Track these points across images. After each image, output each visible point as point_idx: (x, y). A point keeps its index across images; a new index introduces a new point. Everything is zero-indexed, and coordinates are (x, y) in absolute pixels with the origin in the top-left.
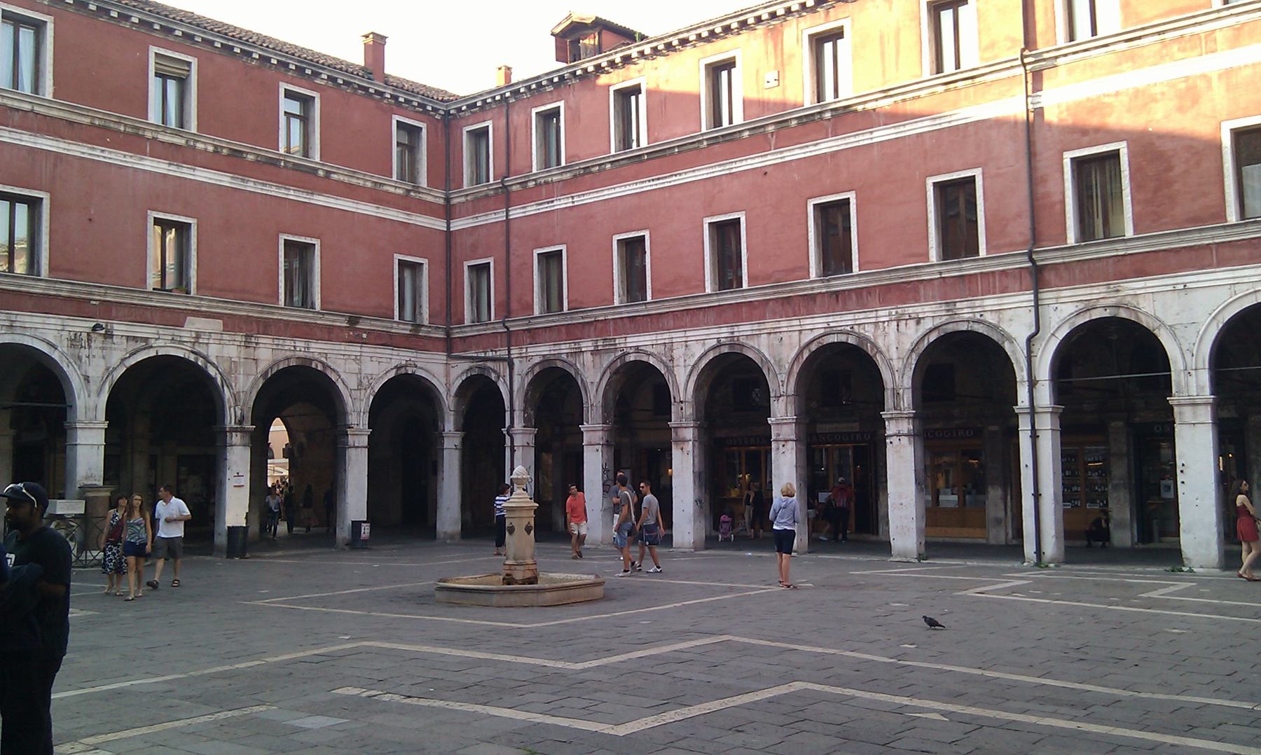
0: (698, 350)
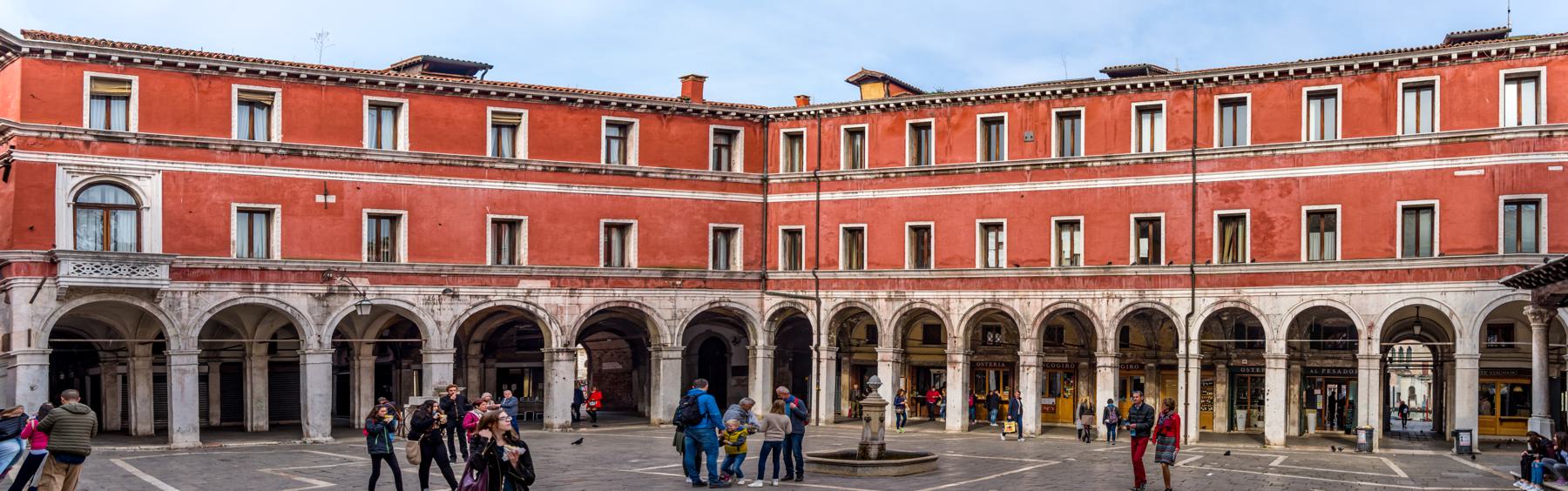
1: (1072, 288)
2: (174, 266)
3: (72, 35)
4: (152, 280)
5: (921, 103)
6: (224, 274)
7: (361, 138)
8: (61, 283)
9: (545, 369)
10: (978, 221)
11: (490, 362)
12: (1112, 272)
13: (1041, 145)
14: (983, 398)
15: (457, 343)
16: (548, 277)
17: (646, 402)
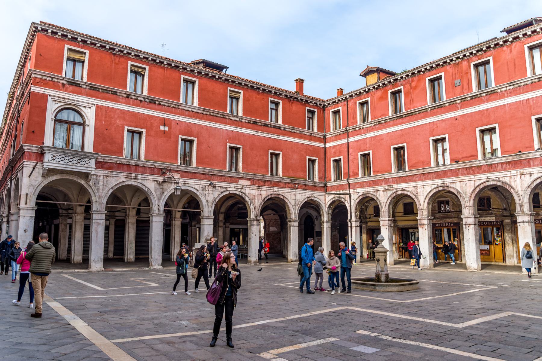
0: (428, 189)
1: (494, 171)
2: (97, 160)
3: (62, 27)
4: (87, 167)
5: (396, 80)
6: (120, 166)
7: (180, 97)
8: (45, 166)
9: (249, 230)
10: (431, 139)
11: (227, 224)
12: (522, 157)
13: (466, 86)
14: (441, 246)
15: (215, 214)
16: (250, 179)
17: (286, 249)
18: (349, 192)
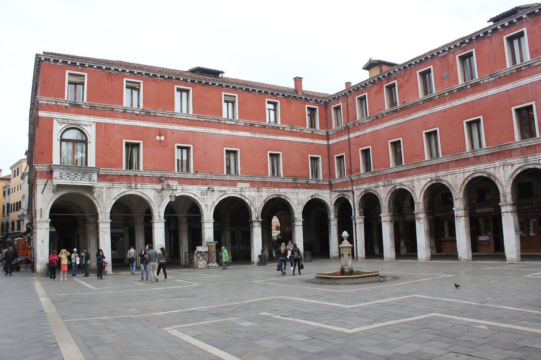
0: (423, 183)
1: (480, 163)
18: (352, 189)
